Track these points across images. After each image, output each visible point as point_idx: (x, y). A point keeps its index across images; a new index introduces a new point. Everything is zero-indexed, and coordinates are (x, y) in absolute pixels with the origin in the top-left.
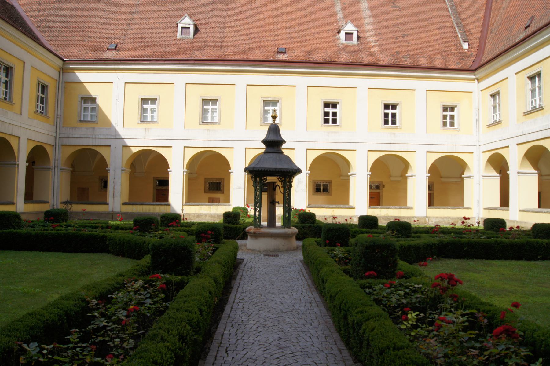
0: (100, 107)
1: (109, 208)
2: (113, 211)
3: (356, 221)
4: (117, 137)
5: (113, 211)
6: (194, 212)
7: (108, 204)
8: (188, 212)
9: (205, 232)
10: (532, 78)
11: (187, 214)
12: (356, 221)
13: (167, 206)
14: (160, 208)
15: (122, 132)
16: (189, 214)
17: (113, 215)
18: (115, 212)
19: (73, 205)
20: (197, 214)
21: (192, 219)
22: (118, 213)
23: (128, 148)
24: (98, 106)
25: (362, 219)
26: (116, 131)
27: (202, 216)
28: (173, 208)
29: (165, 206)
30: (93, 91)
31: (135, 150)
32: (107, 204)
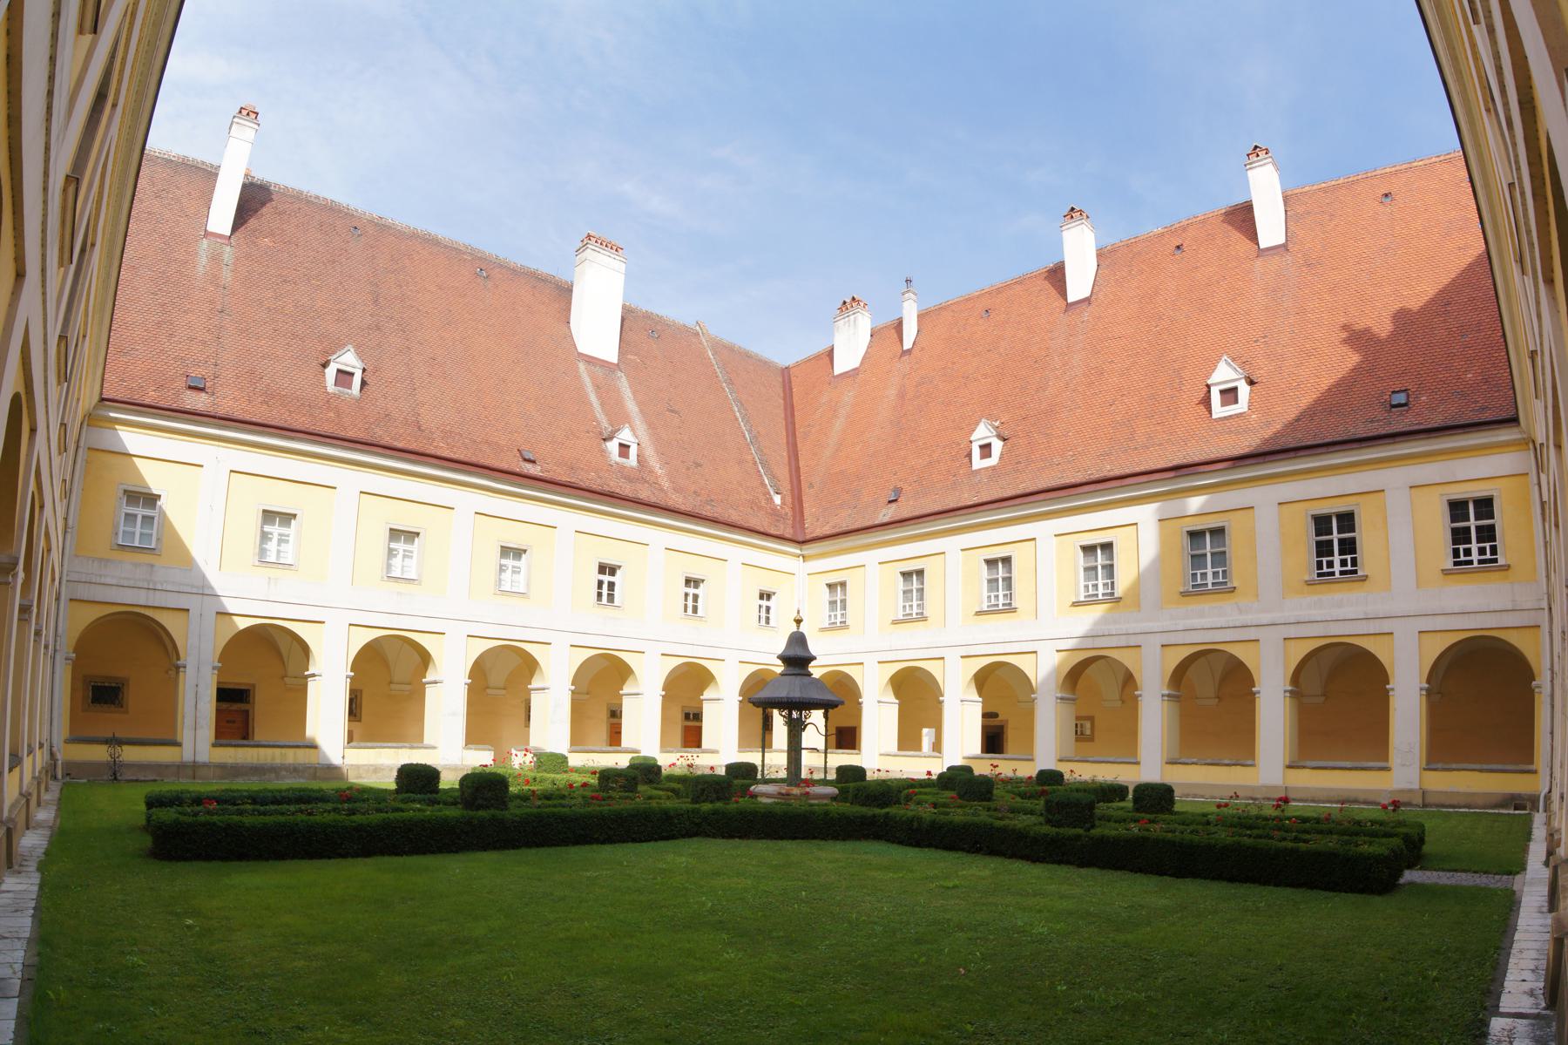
0: (168, 519)
1: (187, 754)
2: (194, 762)
3: (722, 772)
4: (205, 592)
5: (194, 762)
6: (365, 763)
7: (179, 744)
8: (354, 762)
9: (1115, 790)
10: (906, 575)
11: (352, 765)
12: (722, 772)
13: (312, 750)
14: (295, 754)
15: (217, 580)
16: (358, 767)
17: (194, 768)
18: (198, 762)
19: (124, 747)
20: (372, 765)
21: (364, 775)
22: (205, 765)
23: (227, 617)
24: (163, 514)
25: (730, 768)
26: (204, 577)
27: (383, 769)
28: (324, 753)
29: (307, 750)
30: (154, 477)
31: (243, 624)
32: (176, 744)
